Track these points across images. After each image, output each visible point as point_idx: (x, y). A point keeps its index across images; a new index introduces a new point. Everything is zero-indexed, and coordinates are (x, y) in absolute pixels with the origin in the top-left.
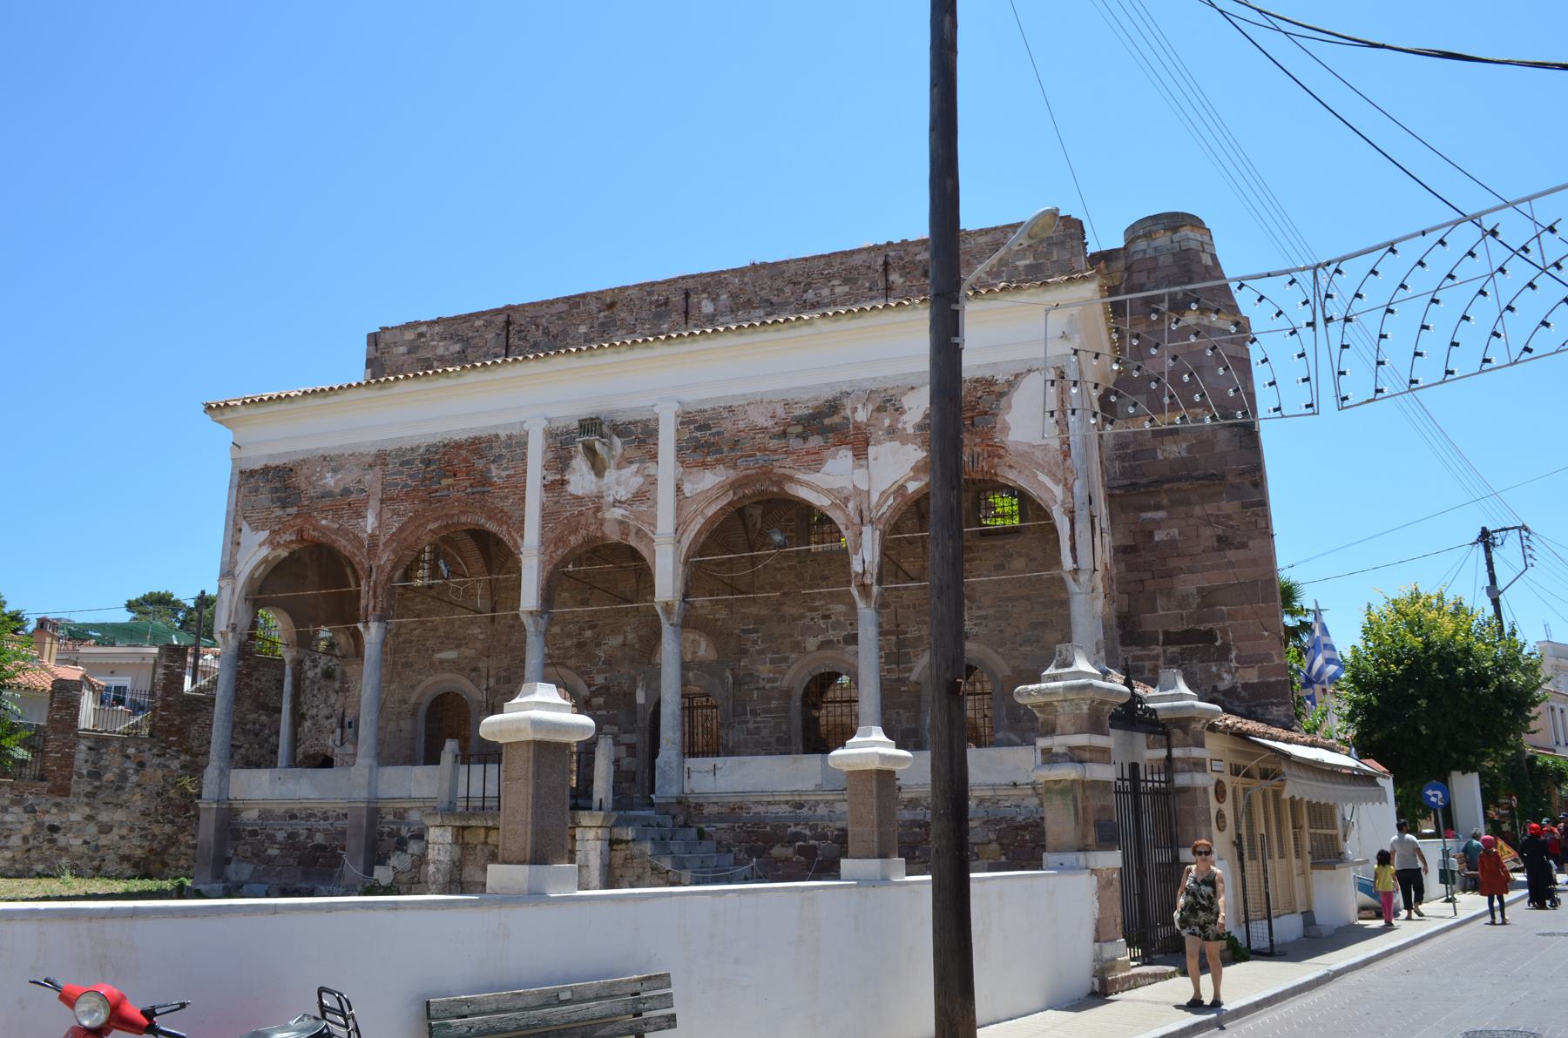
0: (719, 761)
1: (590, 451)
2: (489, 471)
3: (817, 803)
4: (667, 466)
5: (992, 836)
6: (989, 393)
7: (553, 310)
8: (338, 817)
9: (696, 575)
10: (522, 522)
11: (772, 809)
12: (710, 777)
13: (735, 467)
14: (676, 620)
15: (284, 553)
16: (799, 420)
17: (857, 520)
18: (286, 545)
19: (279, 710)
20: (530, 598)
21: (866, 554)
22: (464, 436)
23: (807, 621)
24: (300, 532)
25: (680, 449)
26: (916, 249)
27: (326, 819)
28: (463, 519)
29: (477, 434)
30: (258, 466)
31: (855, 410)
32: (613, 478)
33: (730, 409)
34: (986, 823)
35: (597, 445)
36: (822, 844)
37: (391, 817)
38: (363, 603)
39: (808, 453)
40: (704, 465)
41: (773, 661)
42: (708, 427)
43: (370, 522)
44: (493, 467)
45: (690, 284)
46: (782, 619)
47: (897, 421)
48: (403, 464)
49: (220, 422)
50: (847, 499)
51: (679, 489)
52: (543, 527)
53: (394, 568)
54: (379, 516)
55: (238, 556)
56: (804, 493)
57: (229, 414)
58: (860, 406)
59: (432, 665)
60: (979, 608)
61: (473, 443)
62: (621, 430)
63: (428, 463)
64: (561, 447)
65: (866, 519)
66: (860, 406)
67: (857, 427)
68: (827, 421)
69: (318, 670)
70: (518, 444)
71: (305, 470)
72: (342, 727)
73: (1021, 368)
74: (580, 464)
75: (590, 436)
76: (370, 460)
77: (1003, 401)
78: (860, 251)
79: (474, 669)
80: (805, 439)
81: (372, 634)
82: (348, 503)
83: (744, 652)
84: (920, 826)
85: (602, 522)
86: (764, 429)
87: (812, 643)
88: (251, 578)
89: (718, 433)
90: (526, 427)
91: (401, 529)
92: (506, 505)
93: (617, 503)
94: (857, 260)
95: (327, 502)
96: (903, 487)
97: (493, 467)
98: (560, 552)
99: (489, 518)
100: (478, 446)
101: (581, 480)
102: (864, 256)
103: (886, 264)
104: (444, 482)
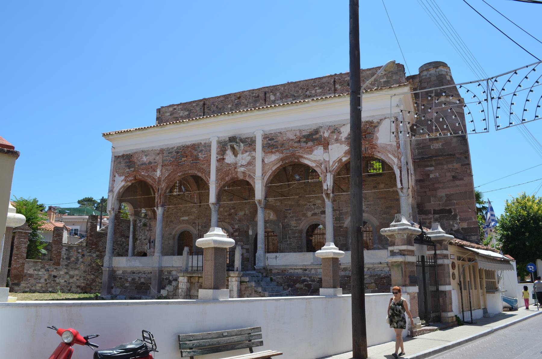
0: (278, 254)
1: (233, 148)
3: (312, 269)
4: (259, 153)
5: (373, 281)
7: (220, 100)
8: (148, 273)
9: (269, 190)
11: (296, 271)
12: (274, 260)
13: (282, 153)
14: (262, 206)
15: (130, 184)
16: (304, 136)
17: (325, 171)
18: (131, 181)
19: (129, 237)
20: (212, 198)
21: (328, 183)
22: (190, 143)
23: (308, 206)
24: (135, 177)
25: (263, 147)
27: (145, 274)
28: (190, 172)
30: (120, 155)
31: (324, 133)
33: (281, 133)
34: (371, 276)
35: (235, 146)
36: (313, 283)
37: (166, 273)
38: (156, 200)
39: (308, 148)
40: (272, 152)
41: (296, 220)
42: (273, 139)
43: (158, 173)
44: (200, 154)
45: (266, 90)
47: (339, 136)
48: (169, 153)
49: (108, 140)
50: (321, 164)
51: (263, 161)
52: (217, 174)
53: (167, 189)
54: (161, 171)
55: (115, 185)
56: (306, 162)
57: (111, 137)
58: (326, 131)
59: (180, 221)
60: (368, 201)
62: (243, 141)
63: (177, 153)
64: (223, 147)
65: (328, 171)
67: (325, 138)
68: (314, 137)
69: (142, 223)
70: (208, 146)
71: (136, 156)
72: (150, 243)
74: (229, 152)
75: (232, 143)
76: (158, 152)
77: (376, 129)
78: (325, 77)
79: (194, 223)
80: (307, 143)
81: (159, 211)
82: (151, 166)
83: (286, 217)
84: (347, 277)
85: (237, 172)
86: (292, 140)
87: (309, 214)
88: (119, 193)
89: (277, 141)
90: (211, 140)
91: (169, 175)
93: (242, 166)
94: (324, 80)
95: (144, 166)
96: (341, 160)
97: (200, 154)
98: (223, 183)
99: (199, 171)
100: (194, 147)
101: (229, 158)
102: (327, 79)
103: (334, 81)
104: (183, 159)
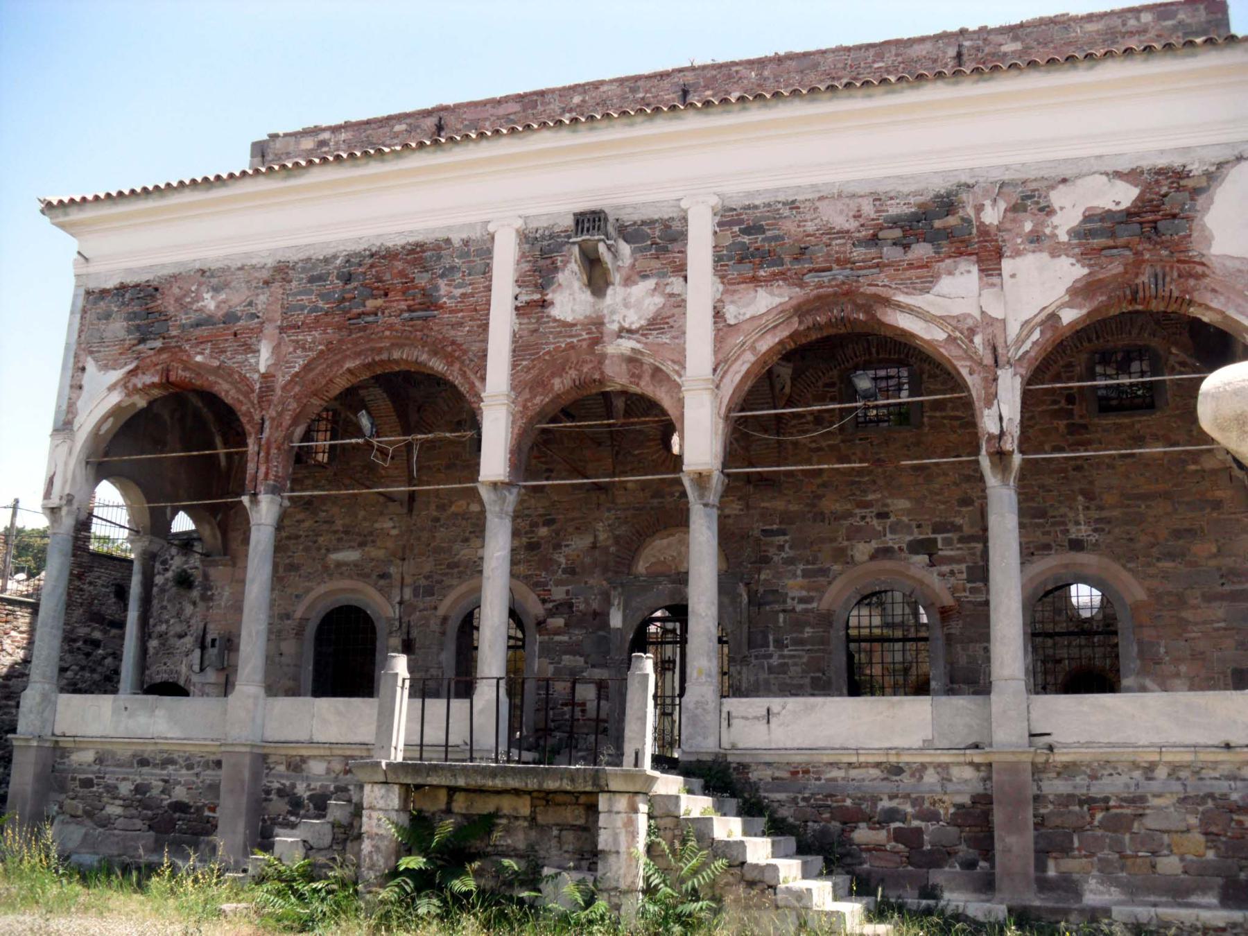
0: (775, 703)
1: (592, 262)
2: (437, 288)
3: (924, 766)
4: (701, 282)
5: (1193, 821)
6: (1178, 190)
7: (501, 111)
8: (207, 765)
9: (744, 433)
10: (484, 356)
11: (853, 773)
12: (761, 726)
13: (801, 285)
14: (713, 498)
15: (141, 403)
16: (895, 222)
17: (988, 360)
18: (147, 388)
19: (121, 625)
20: (495, 460)
21: (1002, 411)
22: (401, 241)
23: (856, 521)
24: (166, 372)
25: (718, 260)
26: (1000, 39)
27: (189, 767)
28: (396, 355)
29: (419, 238)
30: (110, 285)
31: (979, 208)
32: (619, 299)
33: (793, 205)
34: (1183, 800)
35: (602, 248)
36: (930, 827)
37: (282, 768)
38: (251, 467)
39: (911, 266)
40: (755, 280)
41: (806, 574)
42: (759, 229)
43: (264, 358)
44: (442, 283)
45: (690, 78)
46: (820, 517)
47: (1042, 224)
48: (312, 280)
49: (62, 226)
50: (972, 331)
51: (718, 314)
52: (514, 365)
53: (295, 421)
54: (276, 349)
55: (80, 404)
56: (905, 322)
57: (75, 215)
58: (988, 203)
59: (326, 568)
60: (1100, 508)
61: (412, 252)
62: (631, 233)
63: (348, 278)
64: (540, 257)
65: (1002, 360)
66: (988, 203)
67: (984, 231)
68: (937, 224)
69: (170, 574)
70: (478, 254)
71: (176, 291)
72: (203, 648)
73: (1229, 154)
74: (571, 277)
75: (587, 242)
76: (265, 275)
77: (1201, 200)
78: (923, 40)
79: (383, 576)
80: (906, 247)
81: (264, 513)
82: (233, 330)
83: (765, 560)
84: (1081, 803)
85: (602, 357)
86: (844, 233)
87: (862, 550)
88: (95, 434)
89: (775, 238)
90: (491, 228)
91: (307, 368)
92: (460, 335)
93: (624, 332)
94: (917, 51)
95: (203, 331)
96: (1054, 317)
97: (442, 283)
98: (538, 400)
99: (435, 353)
100: (419, 255)
101: (570, 300)
102: (928, 46)
103: (959, 55)
104: (371, 304)
